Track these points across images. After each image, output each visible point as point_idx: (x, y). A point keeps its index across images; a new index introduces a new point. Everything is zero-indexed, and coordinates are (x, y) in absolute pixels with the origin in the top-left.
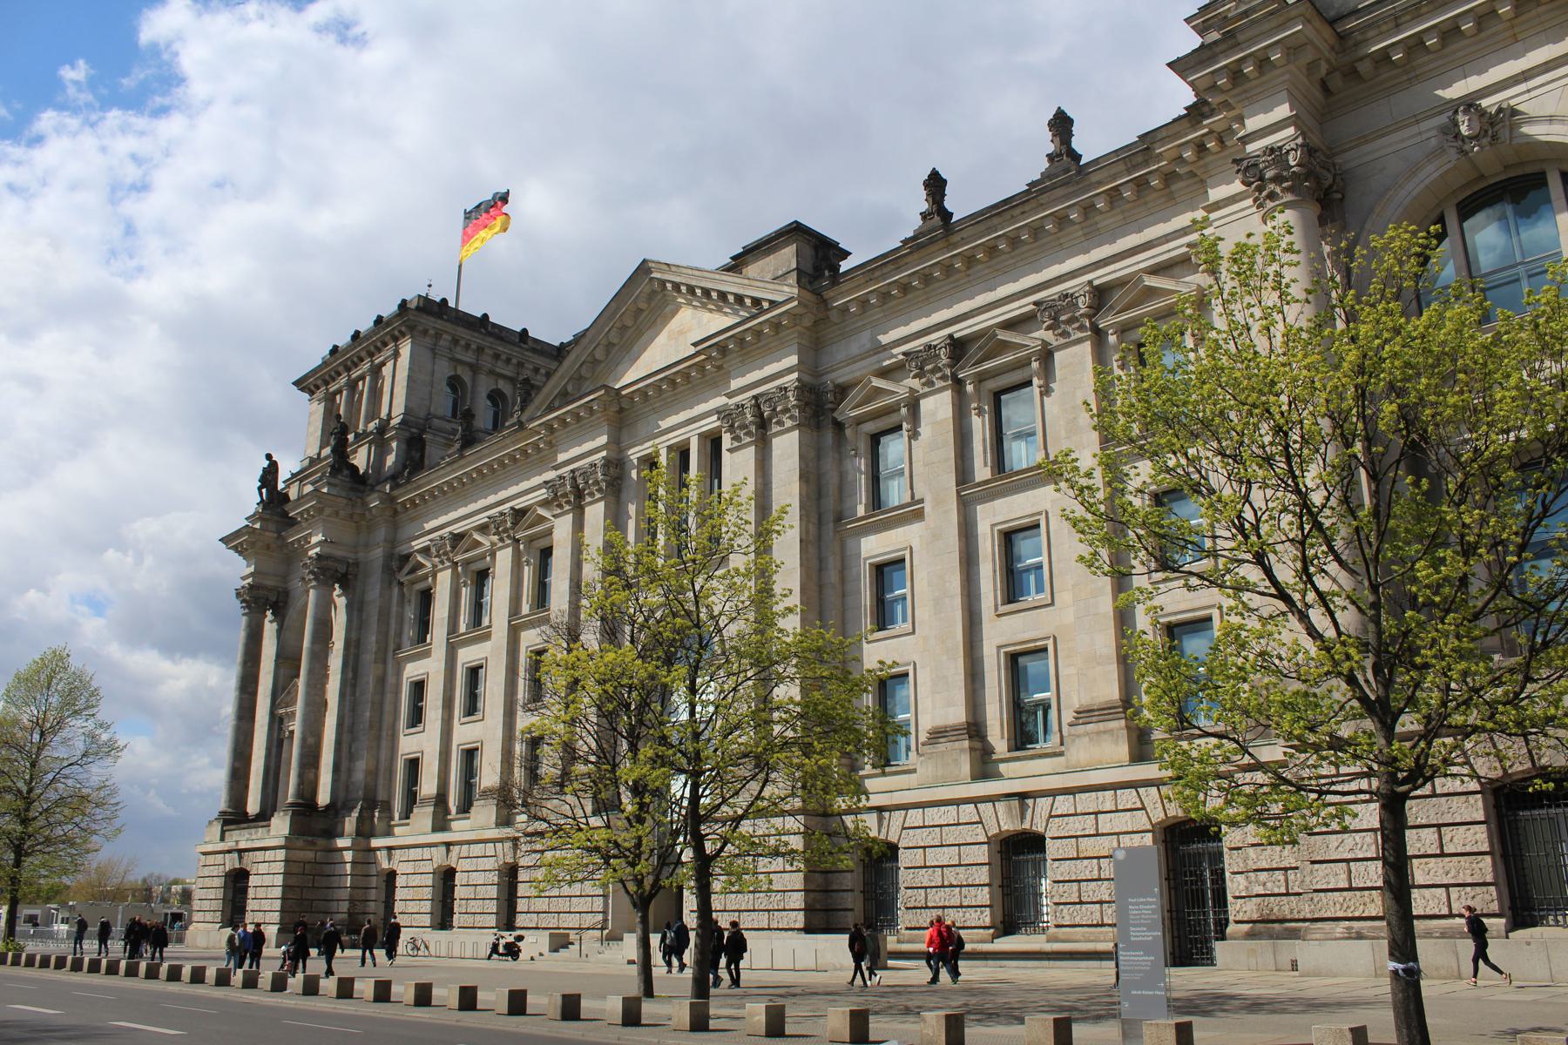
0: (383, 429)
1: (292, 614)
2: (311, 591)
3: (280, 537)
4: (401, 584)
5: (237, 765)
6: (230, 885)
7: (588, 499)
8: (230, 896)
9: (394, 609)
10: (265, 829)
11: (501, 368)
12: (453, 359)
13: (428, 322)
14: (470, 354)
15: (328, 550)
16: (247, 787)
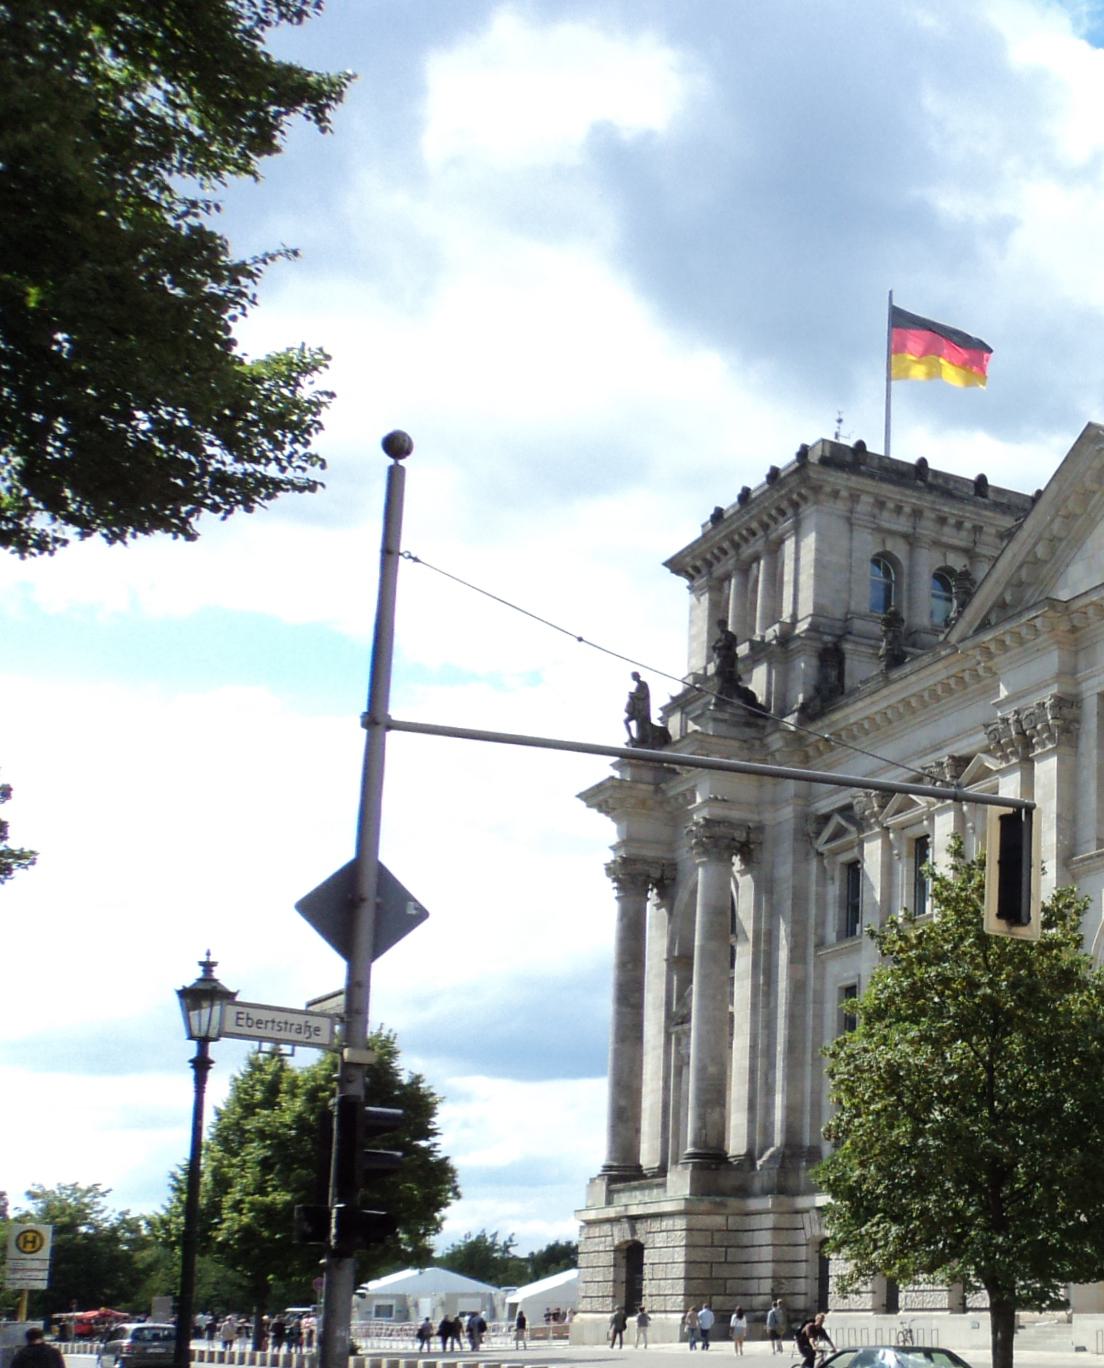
0: (786, 638)
1: (683, 895)
2: (700, 871)
3: (658, 790)
4: (820, 855)
5: (623, 1103)
6: (623, 1262)
7: (1039, 750)
8: (623, 1276)
9: (813, 888)
10: (661, 1190)
11: (949, 535)
12: (879, 530)
13: (838, 479)
14: (903, 520)
15: (719, 812)
16: (638, 1131)
